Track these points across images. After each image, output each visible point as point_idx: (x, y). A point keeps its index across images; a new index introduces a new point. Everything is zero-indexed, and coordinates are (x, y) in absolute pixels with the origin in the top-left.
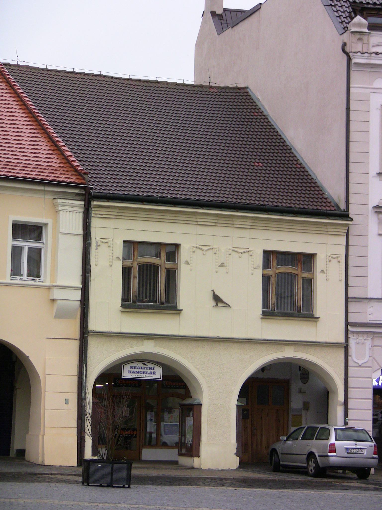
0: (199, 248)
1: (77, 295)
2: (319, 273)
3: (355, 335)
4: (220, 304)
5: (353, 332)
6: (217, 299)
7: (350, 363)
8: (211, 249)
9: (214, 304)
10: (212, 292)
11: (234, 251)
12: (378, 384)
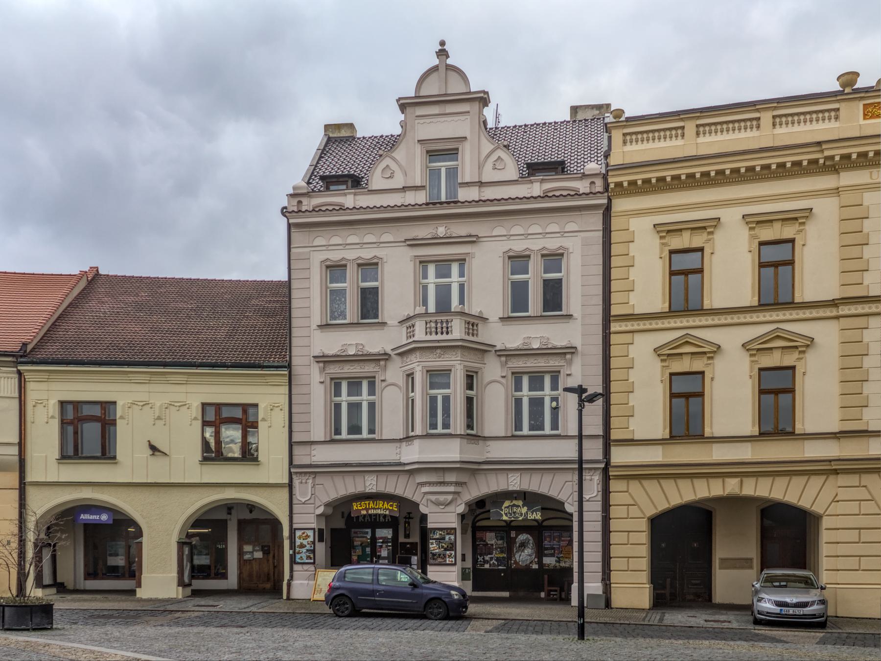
0: (134, 404)
1: (15, 450)
2: (261, 421)
3: (298, 475)
4: (157, 453)
5: (296, 473)
6: (154, 449)
7: (295, 501)
8: (146, 404)
9: (151, 452)
10: (148, 443)
11: (171, 405)
12: (365, 520)
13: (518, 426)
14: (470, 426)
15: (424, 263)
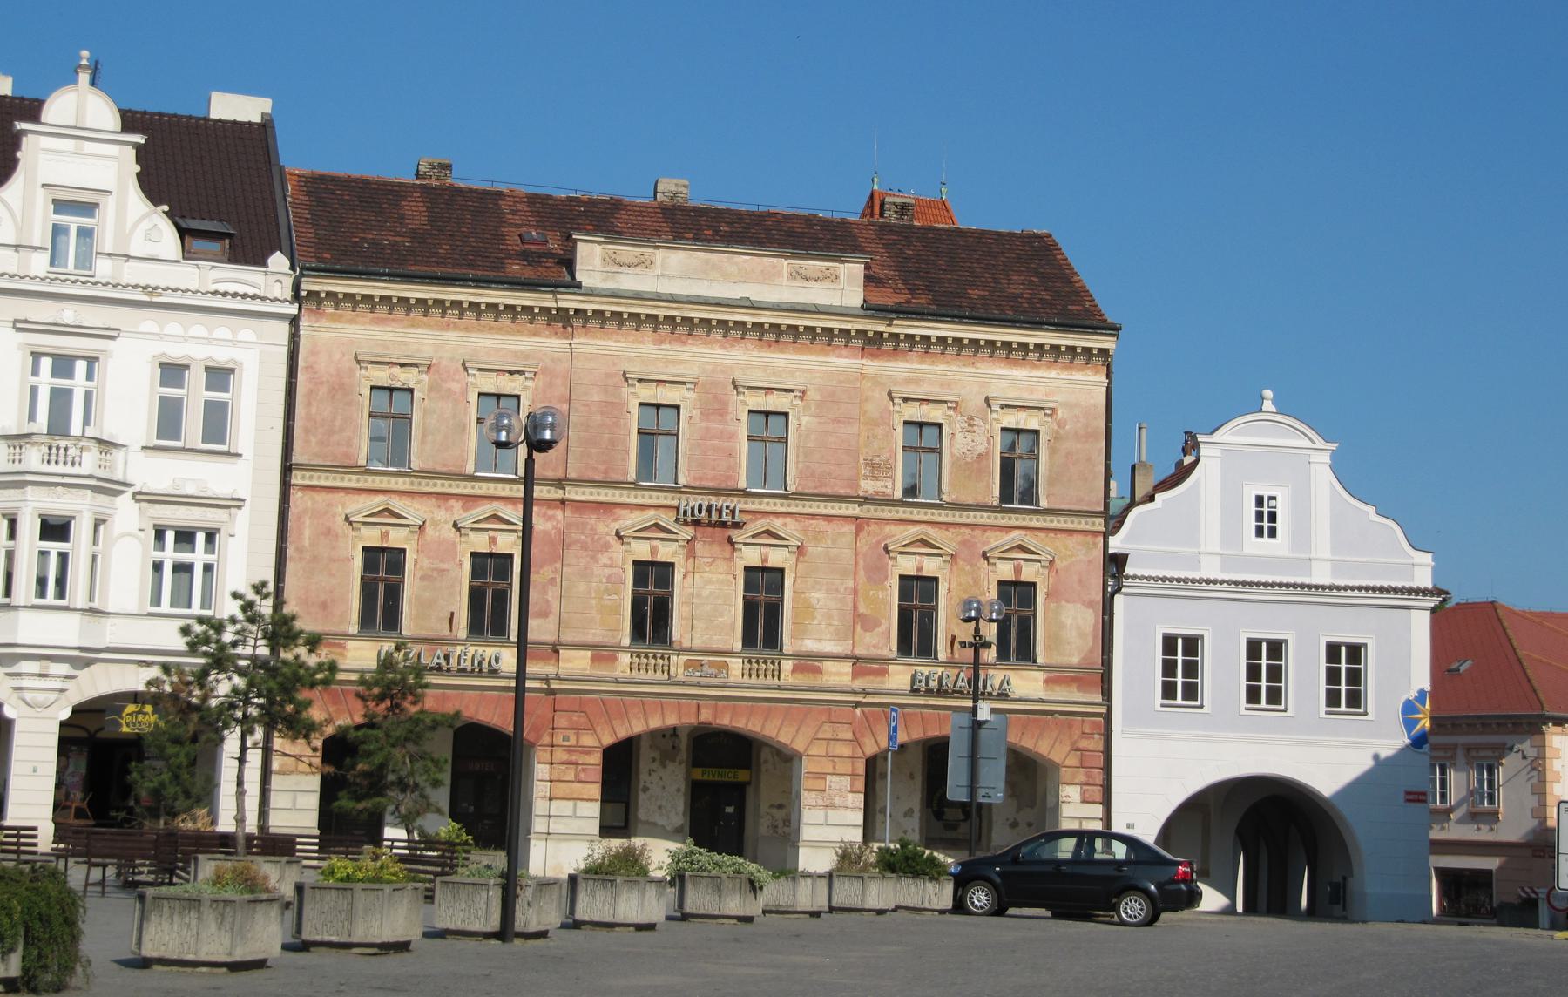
13: (156, 601)
14: (91, 598)
15: (36, 356)
